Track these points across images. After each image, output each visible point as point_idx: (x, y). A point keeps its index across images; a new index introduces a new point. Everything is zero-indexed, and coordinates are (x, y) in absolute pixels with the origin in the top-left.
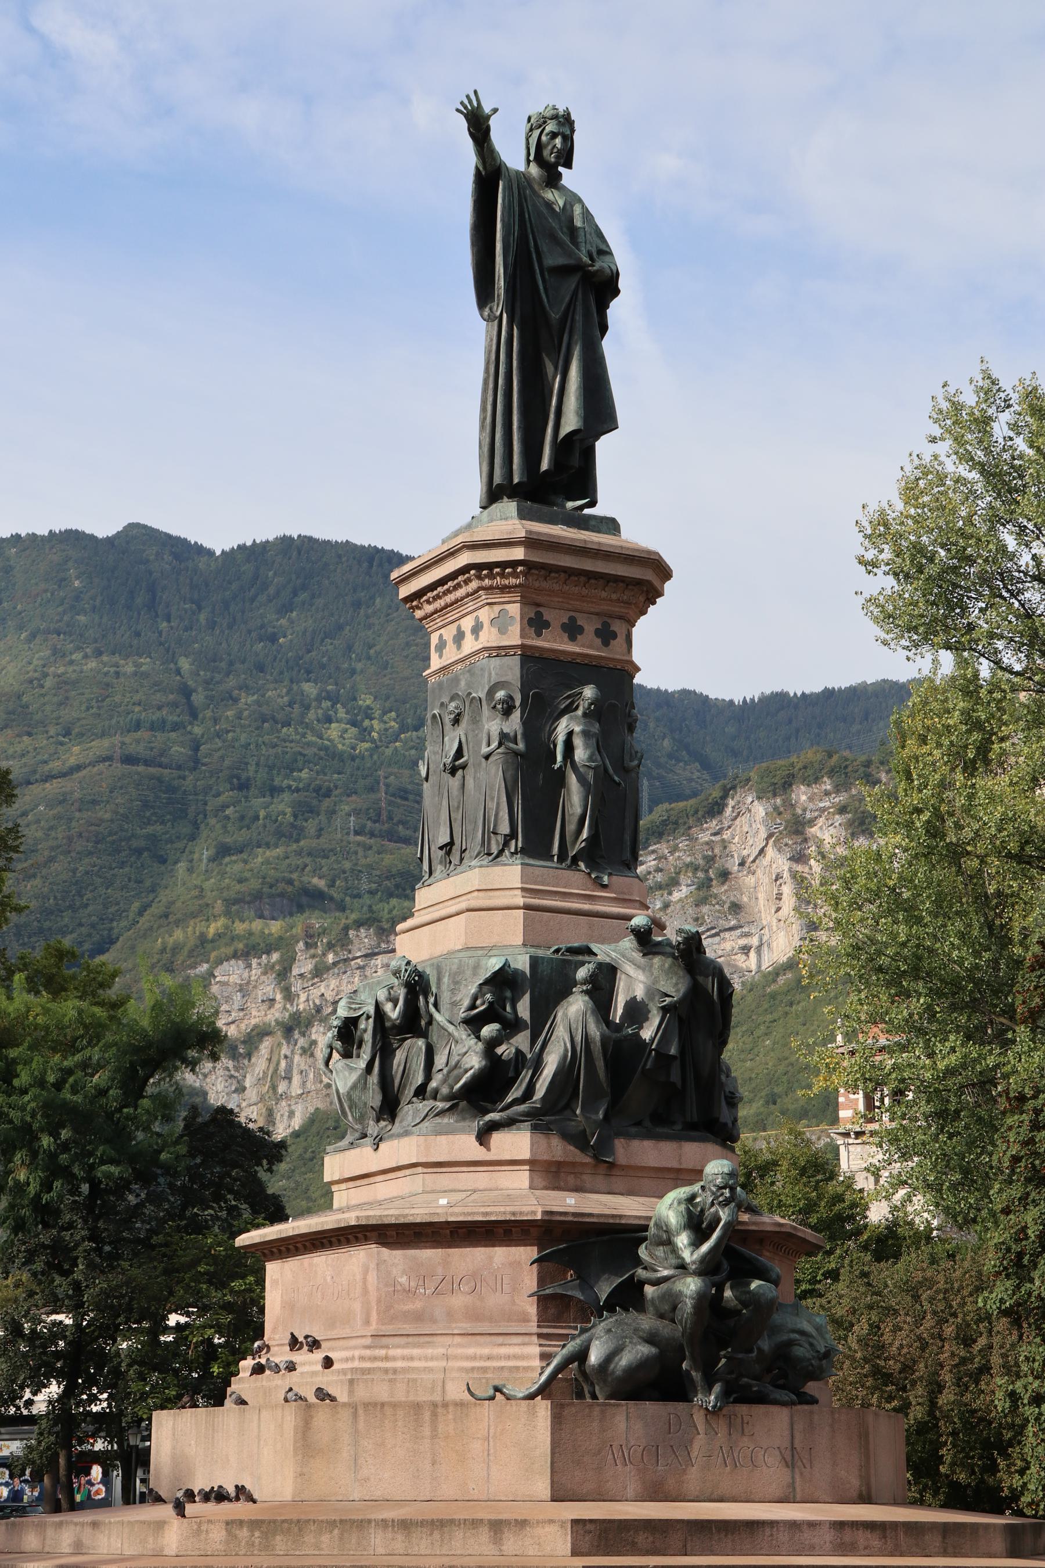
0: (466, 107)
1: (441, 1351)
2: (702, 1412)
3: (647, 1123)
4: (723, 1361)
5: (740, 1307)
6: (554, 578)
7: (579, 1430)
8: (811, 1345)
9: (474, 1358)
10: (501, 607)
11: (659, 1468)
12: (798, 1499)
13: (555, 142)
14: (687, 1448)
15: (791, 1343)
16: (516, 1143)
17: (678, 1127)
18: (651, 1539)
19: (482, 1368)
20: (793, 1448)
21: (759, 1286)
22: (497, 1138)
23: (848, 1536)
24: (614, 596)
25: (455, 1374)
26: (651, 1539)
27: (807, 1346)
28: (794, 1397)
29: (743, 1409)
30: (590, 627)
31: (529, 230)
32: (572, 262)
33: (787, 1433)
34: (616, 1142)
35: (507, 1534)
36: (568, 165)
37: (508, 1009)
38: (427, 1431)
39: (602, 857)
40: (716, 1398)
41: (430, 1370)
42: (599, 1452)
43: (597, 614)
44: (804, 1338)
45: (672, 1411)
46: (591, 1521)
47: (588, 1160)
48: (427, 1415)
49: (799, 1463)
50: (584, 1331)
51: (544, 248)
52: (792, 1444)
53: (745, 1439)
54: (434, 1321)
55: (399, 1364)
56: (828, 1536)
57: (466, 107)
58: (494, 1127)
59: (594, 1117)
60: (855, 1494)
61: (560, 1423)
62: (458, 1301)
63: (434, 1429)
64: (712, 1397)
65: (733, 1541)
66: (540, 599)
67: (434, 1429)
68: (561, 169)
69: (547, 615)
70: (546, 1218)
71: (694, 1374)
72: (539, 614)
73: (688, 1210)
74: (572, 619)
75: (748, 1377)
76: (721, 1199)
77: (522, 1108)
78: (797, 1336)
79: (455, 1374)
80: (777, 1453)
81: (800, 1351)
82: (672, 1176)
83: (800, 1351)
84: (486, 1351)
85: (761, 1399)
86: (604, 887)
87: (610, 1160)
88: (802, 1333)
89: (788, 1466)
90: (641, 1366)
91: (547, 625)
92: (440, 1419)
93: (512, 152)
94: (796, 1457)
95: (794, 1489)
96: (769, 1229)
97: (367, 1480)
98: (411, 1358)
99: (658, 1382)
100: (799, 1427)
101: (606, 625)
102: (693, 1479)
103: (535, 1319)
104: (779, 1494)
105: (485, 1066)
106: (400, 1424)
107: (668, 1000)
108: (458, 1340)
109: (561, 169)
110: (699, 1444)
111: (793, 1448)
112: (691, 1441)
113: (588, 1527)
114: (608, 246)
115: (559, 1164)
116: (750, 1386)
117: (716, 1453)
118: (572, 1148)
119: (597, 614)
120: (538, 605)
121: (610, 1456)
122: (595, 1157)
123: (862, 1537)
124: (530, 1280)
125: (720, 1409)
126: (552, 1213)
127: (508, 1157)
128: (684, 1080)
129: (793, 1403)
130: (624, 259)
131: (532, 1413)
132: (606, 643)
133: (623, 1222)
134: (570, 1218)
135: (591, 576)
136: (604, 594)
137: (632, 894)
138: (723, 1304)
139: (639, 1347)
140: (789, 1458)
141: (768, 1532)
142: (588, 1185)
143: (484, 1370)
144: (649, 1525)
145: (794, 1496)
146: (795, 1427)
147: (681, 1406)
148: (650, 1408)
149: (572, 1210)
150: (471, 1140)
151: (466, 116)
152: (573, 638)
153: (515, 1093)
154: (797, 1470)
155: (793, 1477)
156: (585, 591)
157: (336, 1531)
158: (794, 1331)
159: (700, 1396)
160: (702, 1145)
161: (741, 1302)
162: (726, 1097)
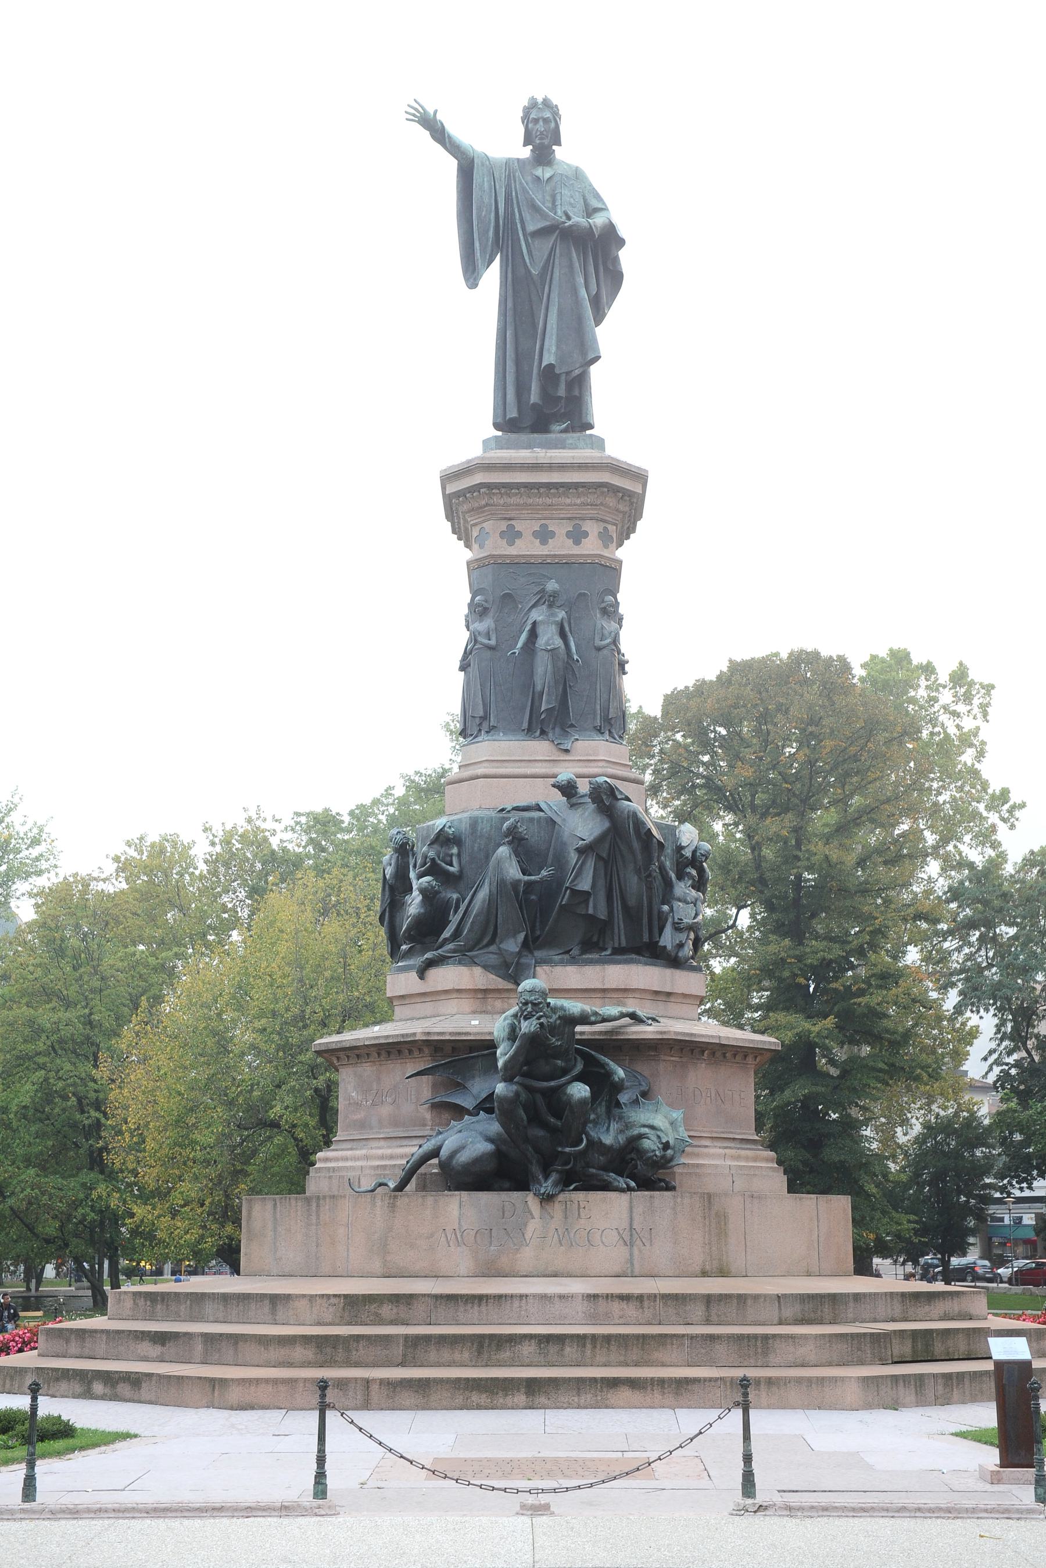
0: (414, 115)
1: (364, 1152)
3: (575, 952)
6: (516, 494)
7: (411, 1217)
8: (659, 1137)
9: (382, 1157)
10: (479, 527)
11: (492, 1248)
12: (637, 1272)
13: (542, 128)
14: (522, 1228)
15: (641, 1136)
16: (449, 976)
17: (608, 952)
18: (395, 1311)
19: (382, 1166)
22: (433, 973)
23: (602, 1306)
24: (578, 501)
25: (368, 1172)
26: (395, 1311)
27: (654, 1138)
28: (633, 1184)
29: (581, 1195)
30: (561, 529)
31: (515, 206)
32: (548, 223)
33: (625, 1215)
35: (280, 1307)
36: (558, 143)
38: (314, 1218)
39: (572, 726)
41: (353, 1168)
42: (432, 1235)
43: (569, 519)
44: (653, 1132)
46: (335, 1296)
48: (314, 1205)
49: (639, 1242)
50: (440, 1133)
51: (527, 216)
52: (631, 1225)
53: (582, 1221)
54: (371, 1128)
55: (341, 1164)
56: (580, 1308)
57: (414, 115)
58: (430, 964)
60: (698, 1269)
61: (394, 1211)
62: (385, 1110)
63: (318, 1216)
65: (480, 1312)
66: (512, 514)
67: (318, 1216)
68: (554, 147)
69: (519, 526)
70: (424, 1038)
72: (511, 527)
74: (577, 527)
77: (450, 946)
78: (646, 1130)
79: (368, 1172)
80: (615, 1233)
81: (647, 1144)
82: (599, 995)
83: (649, 1144)
84: (389, 1151)
85: (606, 1187)
86: (567, 751)
88: (652, 1127)
89: (625, 1244)
90: (477, 1161)
91: (519, 535)
92: (322, 1209)
93: (503, 143)
94: (635, 1236)
95: (632, 1264)
97: (280, 1259)
98: (346, 1159)
99: (498, 1173)
100: (638, 1210)
101: (577, 527)
102: (527, 1257)
103: (430, 1123)
104: (617, 1269)
105: (424, 914)
106: (299, 1213)
107: (581, 842)
108: (382, 1143)
109: (554, 147)
110: (533, 1227)
111: (631, 1228)
112: (525, 1225)
113: (333, 1300)
114: (604, 203)
115: (485, 991)
117: (551, 1234)
118: (494, 977)
119: (569, 519)
120: (510, 519)
121: (443, 1239)
123: (616, 1307)
124: (426, 1093)
126: (429, 1033)
127: (440, 989)
128: (611, 913)
129: (629, 1189)
130: (621, 213)
131: (374, 1204)
132: (577, 542)
134: (447, 1037)
135: (549, 486)
136: (568, 501)
137: (597, 755)
140: (627, 1238)
141: (516, 1303)
143: (384, 1167)
144: (396, 1299)
145: (632, 1271)
146: (634, 1210)
147: (516, 1196)
148: (485, 1198)
149: (475, 1030)
150: (414, 975)
151: (418, 122)
152: (544, 542)
153: (447, 934)
154: (635, 1248)
155: (631, 1255)
156: (549, 501)
157: (188, 1302)
158: (644, 1126)
162: (674, 923)
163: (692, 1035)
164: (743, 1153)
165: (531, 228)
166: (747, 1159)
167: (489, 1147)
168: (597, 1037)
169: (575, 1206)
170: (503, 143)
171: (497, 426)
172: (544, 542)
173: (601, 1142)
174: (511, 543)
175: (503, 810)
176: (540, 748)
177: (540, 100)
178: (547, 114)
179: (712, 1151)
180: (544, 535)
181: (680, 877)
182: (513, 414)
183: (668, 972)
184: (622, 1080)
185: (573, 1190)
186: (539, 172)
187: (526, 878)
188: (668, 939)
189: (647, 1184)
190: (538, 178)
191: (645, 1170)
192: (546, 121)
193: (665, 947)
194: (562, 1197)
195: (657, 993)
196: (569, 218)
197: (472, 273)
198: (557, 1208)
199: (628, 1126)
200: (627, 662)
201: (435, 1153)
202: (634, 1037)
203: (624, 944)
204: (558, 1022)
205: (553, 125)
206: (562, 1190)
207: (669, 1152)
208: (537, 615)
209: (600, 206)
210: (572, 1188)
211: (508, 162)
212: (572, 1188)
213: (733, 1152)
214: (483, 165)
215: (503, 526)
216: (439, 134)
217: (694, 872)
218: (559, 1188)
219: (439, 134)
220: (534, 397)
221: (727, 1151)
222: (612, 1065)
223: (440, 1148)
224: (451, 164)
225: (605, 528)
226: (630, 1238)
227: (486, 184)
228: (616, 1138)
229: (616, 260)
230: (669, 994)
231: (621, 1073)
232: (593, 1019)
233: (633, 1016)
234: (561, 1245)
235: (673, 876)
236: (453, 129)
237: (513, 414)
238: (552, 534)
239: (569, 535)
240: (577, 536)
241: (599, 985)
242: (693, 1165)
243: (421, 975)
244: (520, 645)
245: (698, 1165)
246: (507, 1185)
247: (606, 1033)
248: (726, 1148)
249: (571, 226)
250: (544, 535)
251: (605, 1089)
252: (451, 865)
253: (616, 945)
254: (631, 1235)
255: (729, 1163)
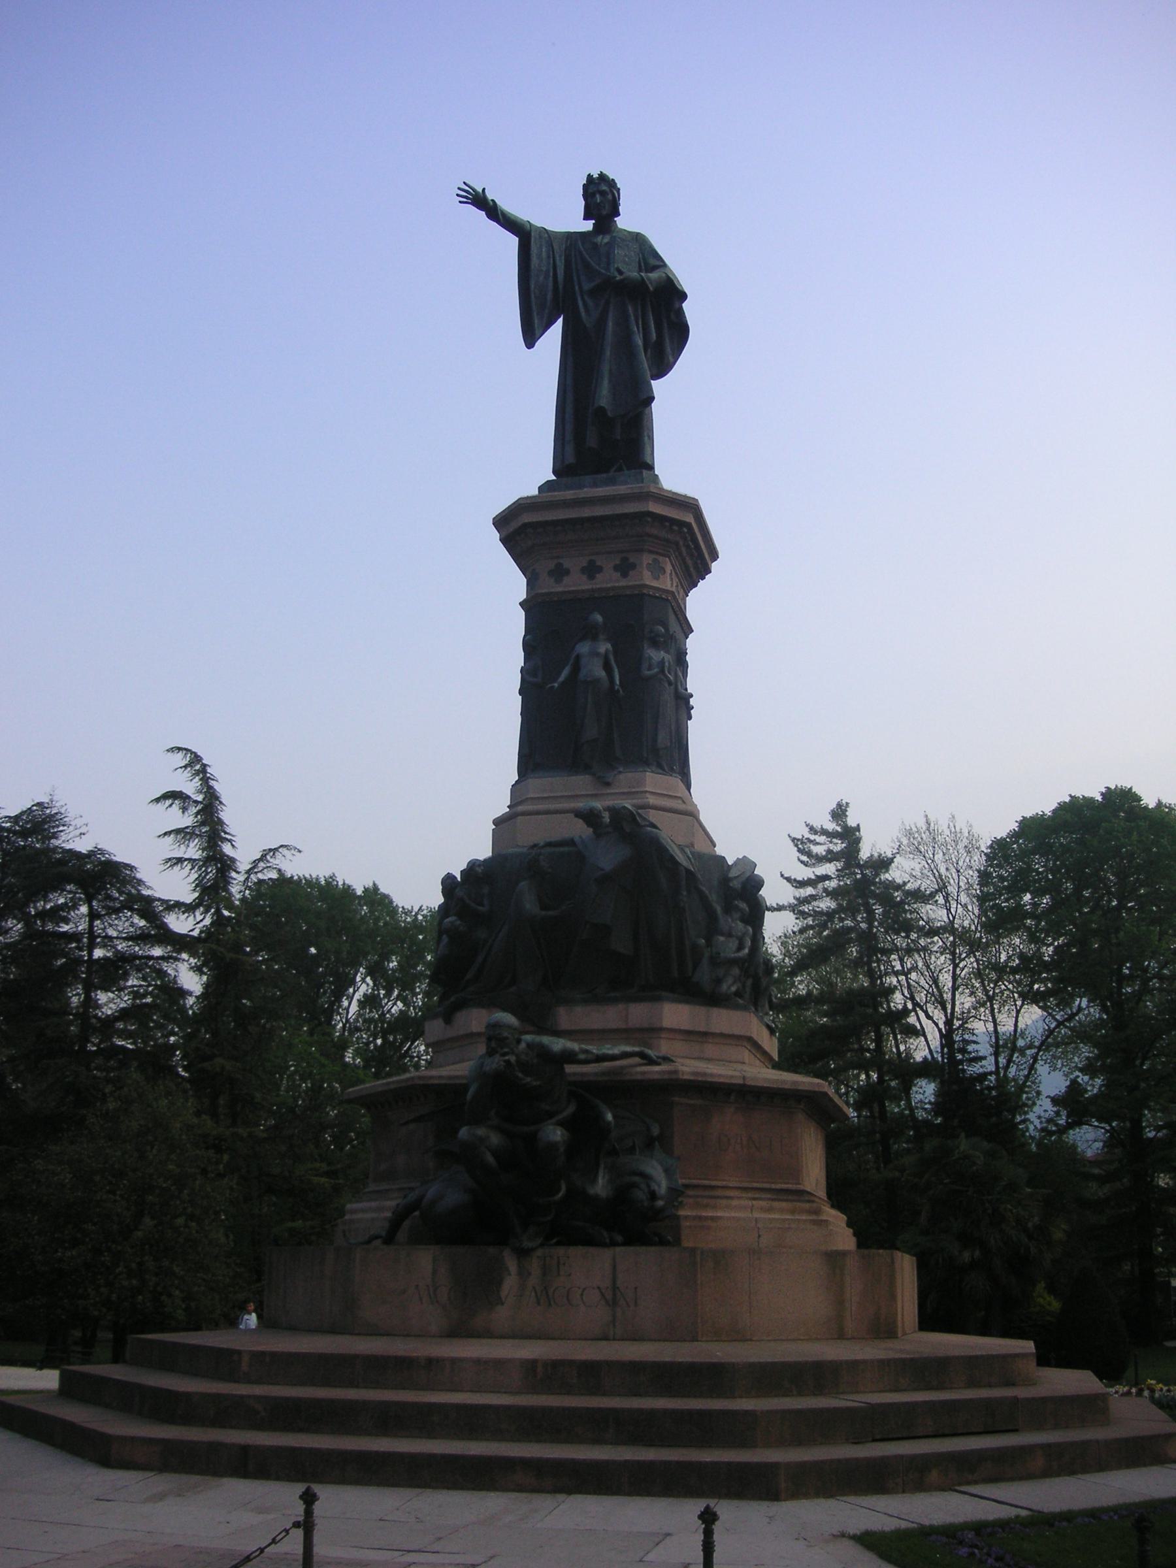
20: (615, 1288)
28: (619, 1239)
29: (561, 1251)
37: (486, 902)
69: (567, 563)
78: (637, 1179)
93: (567, 216)
96: (656, 1077)
101: (625, 560)
102: (502, 1315)
110: (510, 1284)
111: (615, 1288)
114: (663, 261)
120: (558, 557)
129: (614, 1244)
130: (681, 266)
140: (609, 1297)
152: (591, 577)
153: (469, 976)
163: (705, 1074)
164: (776, 1204)
165: (587, 286)
166: (782, 1211)
170: (567, 216)
171: (554, 472)
172: (591, 577)
174: (559, 580)
175: (535, 846)
176: (581, 783)
177: (596, 176)
178: (604, 188)
179: (735, 1203)
180: (591, 570)
181: (728, 909)
182: (571, 459)
184: (609, 1123)
185: (558, 1244)
186: (599, 239)
187: (543, 913)
188: (704, 975)
189: (635, 1238)
190: (596, 244)
191: (638, 1222)
192: (603, 193)
194: (539, 1252)
195: (688, 1033)
196: (620, 272)
197: (530, 337)
198: (534, 1265)
200: (691, 696)
201: (415, 1205)
202: (639, 1077)
204: (535, 1061)
205: (610, 197)
206: (542, 1245)
207: (660, 1203)
208: (584, 648)
209: (658, 263)
210: (554, 1241)
211: (570, 236)
212: (554, 1241)
213: (763, 1203)
214: (540, 237)
215: (552, 565)
216: (493, 212)
217: (743, 906)
218: (539, 1241)
219: (493, 212)
220: (592, 441)
221: (754, 1202)
222: (603, 1107)
223: (422, 1197)
224: (513, 241)
225: (655, 560)
226: (613, 1297)
227: (544, 255)
229: (680, 313)
230: (705, 1034)
232: (582, 1056)
233: (642, 1055)
234: (539, 1303)
235: (719, 910)
236: (506, 205)
237: (571, 459)
238: (600, 569)
239: (616, 568)
240: (625, 568)
241: (621, 1025)
242: (707, 1218)
243: (448, 1020)
244: (561, 679)
245: (713, 1219)
248: (754, 1199)
249: (622, 281)
250: (591, 570)
251: (587, 1135)
252: (483, 905)
254: (614, 1295)
255: (757, 1215)
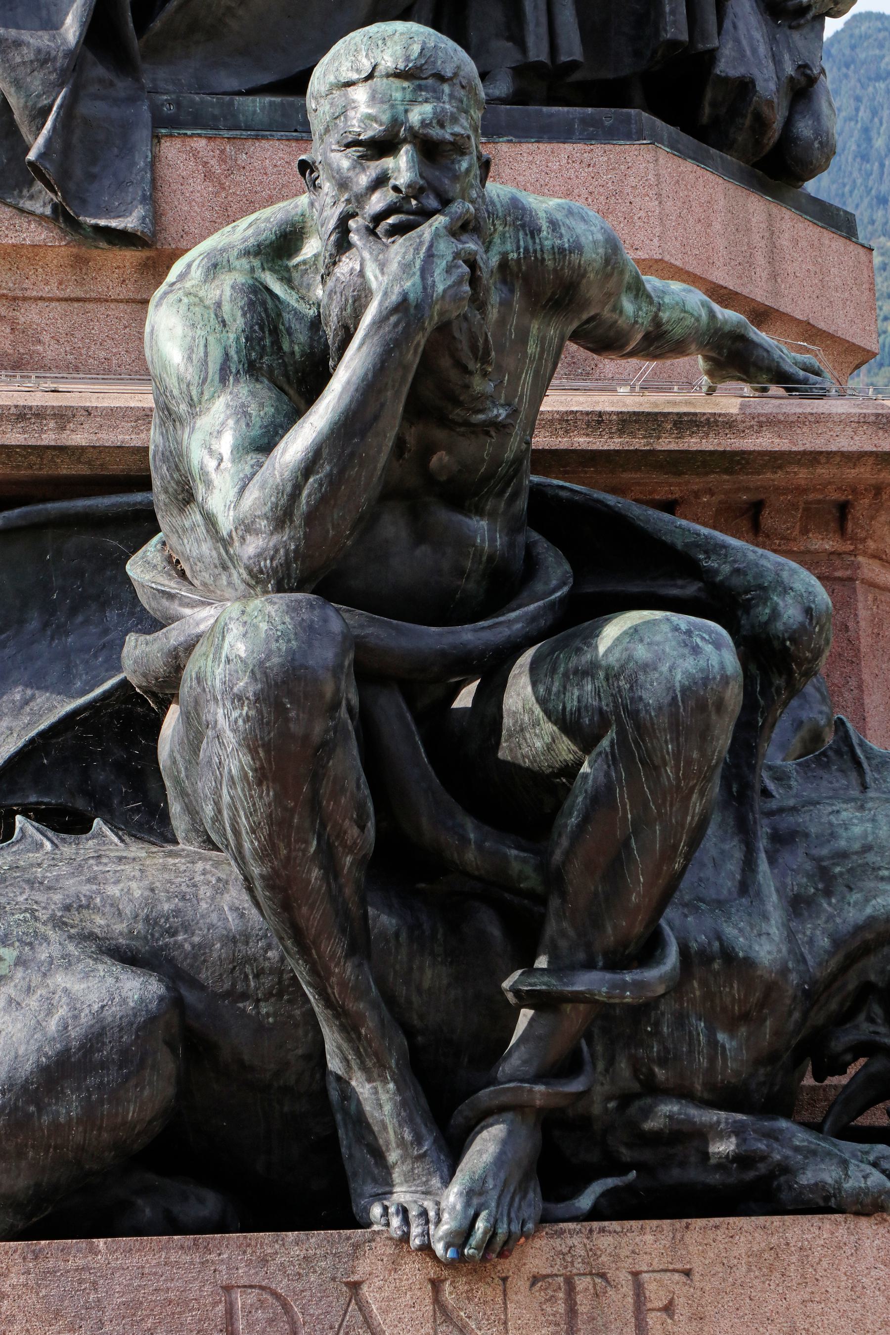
2: (414, 1271)
4: (526, 1015)
5: (566, 749)
21: (634, 632)
29: (646, 1243)
34: (172, 150)
40: (470, 1194)
45: (243, 1275)
47: (35, 234)
59: (36, 40)
64: (453, 1196)
71: (362, 1087)
73: (258, 299)
75: (684, 1094)
76: (377, 202)
85: (757, 1192)
87: (130, 222)
96: (845, 443)
116: (700, 1136)
122: (64, 218)
125: (498, 1247)
133: (78, 438)
138: (503, 754)
139: (60, 980)
142: (49, 350)
147: (291, 1252)
159: (402, 1194)
160: (601, 154)
161: (568, 724)
167: (137, 989)
168: (581, 442)
169: (621, 1298)
173: (728, 955)
183: (757, 207)
185: (595, 1214)
188: (747, 48)
193: (745, 86)
194: (540, 1254)
199: (831, 876)
203: (572, 47)
206: (546, 1219)
210: (585, 1201)
212: (585, 1201)
218: (534, 1195)
228: (791, 937)
231: (805, 581)
246: (210, 1203)
247: (628, 421)
253: (538, 52)
